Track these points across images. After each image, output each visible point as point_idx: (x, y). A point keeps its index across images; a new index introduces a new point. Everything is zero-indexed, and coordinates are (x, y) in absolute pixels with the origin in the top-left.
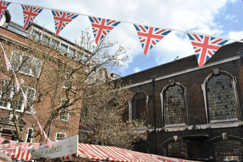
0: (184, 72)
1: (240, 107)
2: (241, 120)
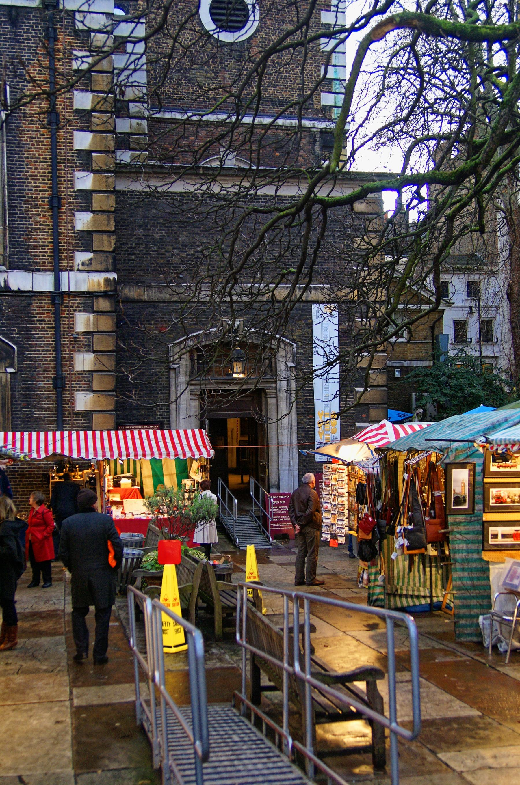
1: (9, 213)
2: (4, 265)
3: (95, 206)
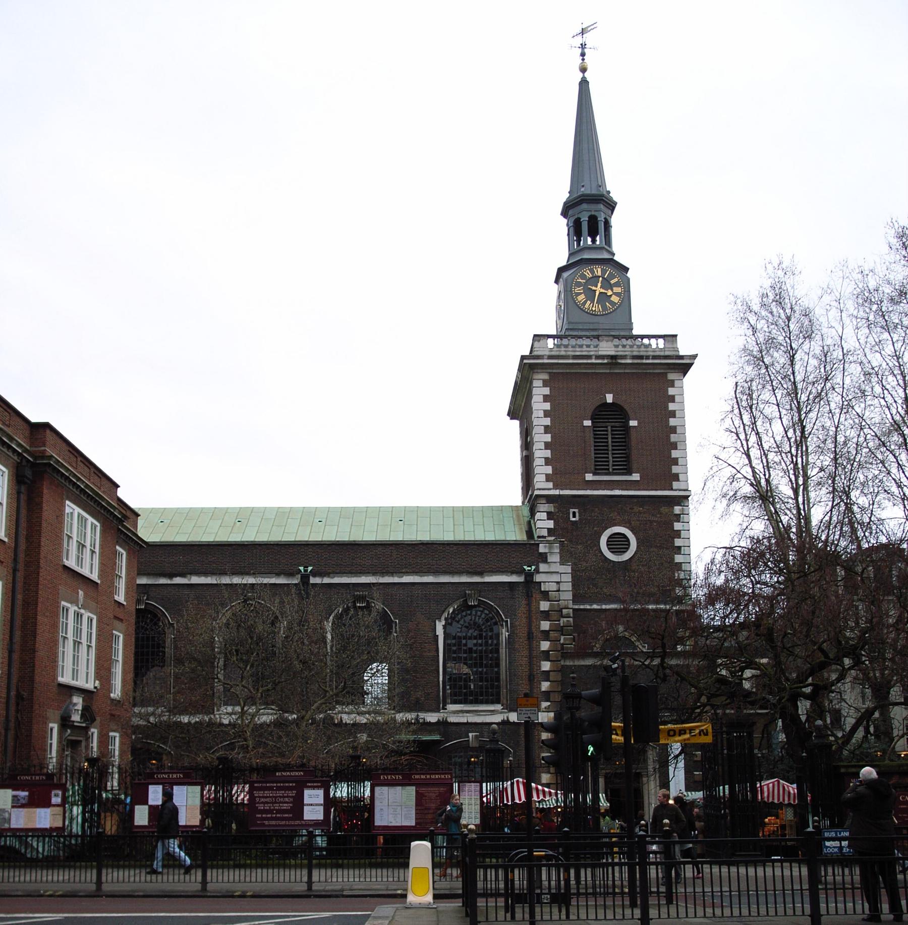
0: (396, 580)
3: (551, 679)
